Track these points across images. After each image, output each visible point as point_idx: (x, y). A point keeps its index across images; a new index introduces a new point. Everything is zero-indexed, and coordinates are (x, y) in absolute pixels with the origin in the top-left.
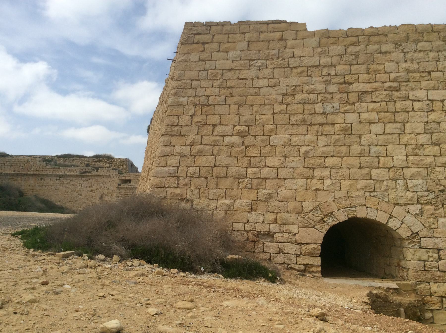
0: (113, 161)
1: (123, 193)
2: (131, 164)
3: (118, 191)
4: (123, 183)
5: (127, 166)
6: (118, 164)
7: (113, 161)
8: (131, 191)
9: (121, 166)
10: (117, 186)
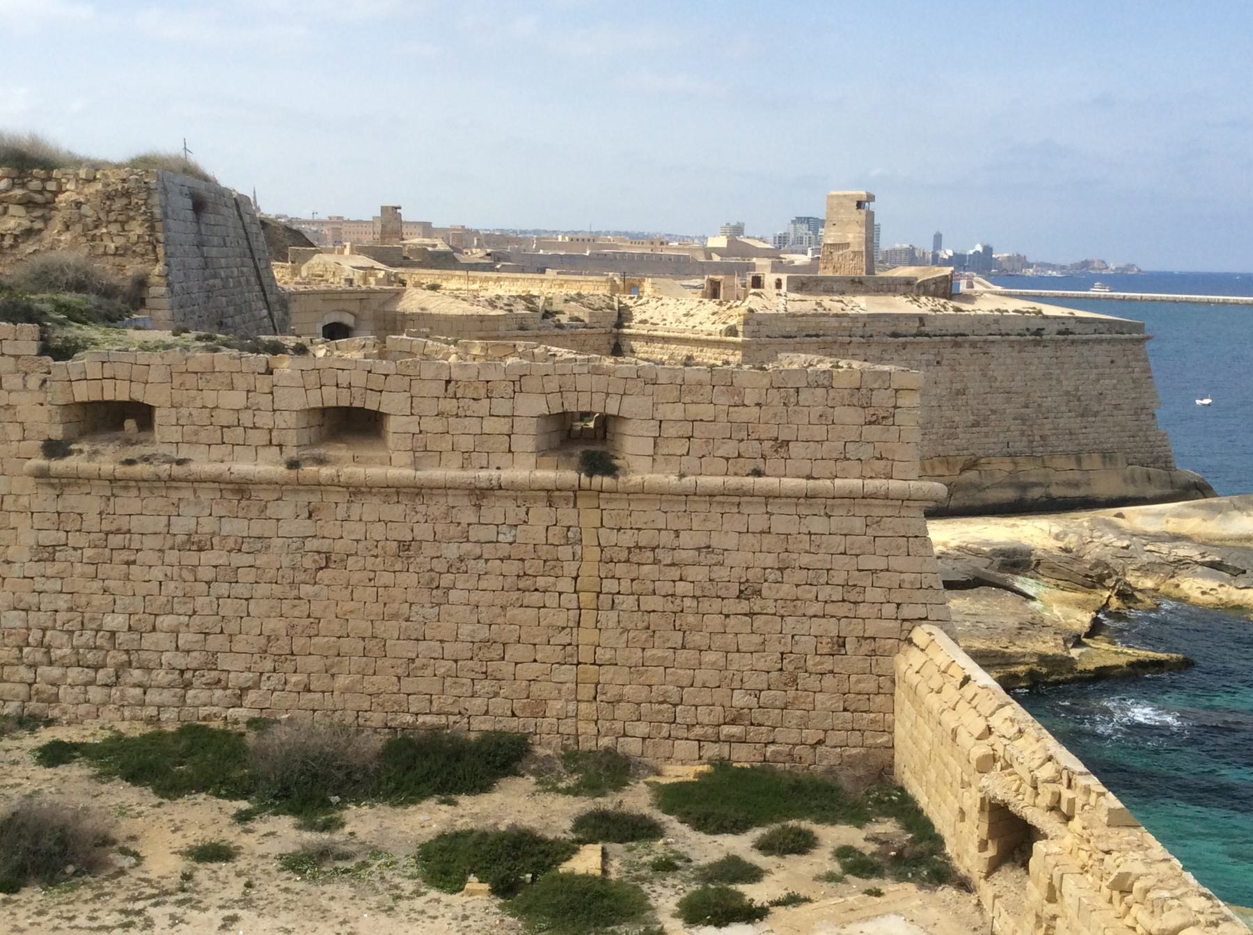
0: (51, 186)
1: (92, 521)
2: (188, 203)
3: (44, 500)
4: (82, 435)
5: (152, 228)
6: (85, 209)
7: (51, 186)
8: (154, 503)
9: (114, 228)
10: (40, 462)
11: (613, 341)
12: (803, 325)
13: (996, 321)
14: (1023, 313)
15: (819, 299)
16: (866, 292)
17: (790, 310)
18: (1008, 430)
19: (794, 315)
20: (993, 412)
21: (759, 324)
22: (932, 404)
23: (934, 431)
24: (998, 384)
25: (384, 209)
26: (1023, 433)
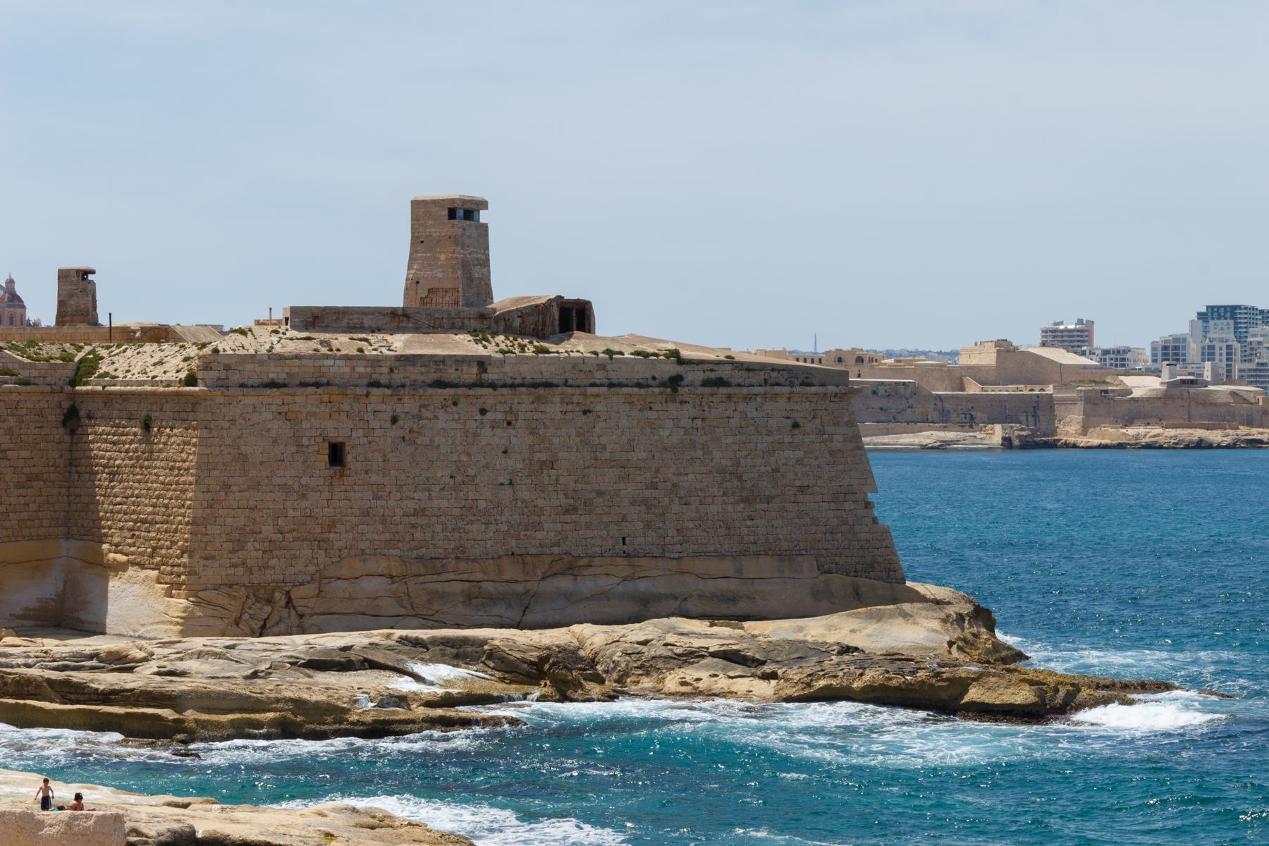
11: (66, 405)
12: (295, 370)
13: (602, 367)
14: (646, 355)
15: (327, 336)
16: (417, 329)
17: (278, 349)
18: (624, 519)
19: (281, 357)
20: (600, 493)
21: (227, 368)
22: (501, 480)
23: (504, 519)
24: (607, 455)
25: (64, 275)
26: (648, 525)
